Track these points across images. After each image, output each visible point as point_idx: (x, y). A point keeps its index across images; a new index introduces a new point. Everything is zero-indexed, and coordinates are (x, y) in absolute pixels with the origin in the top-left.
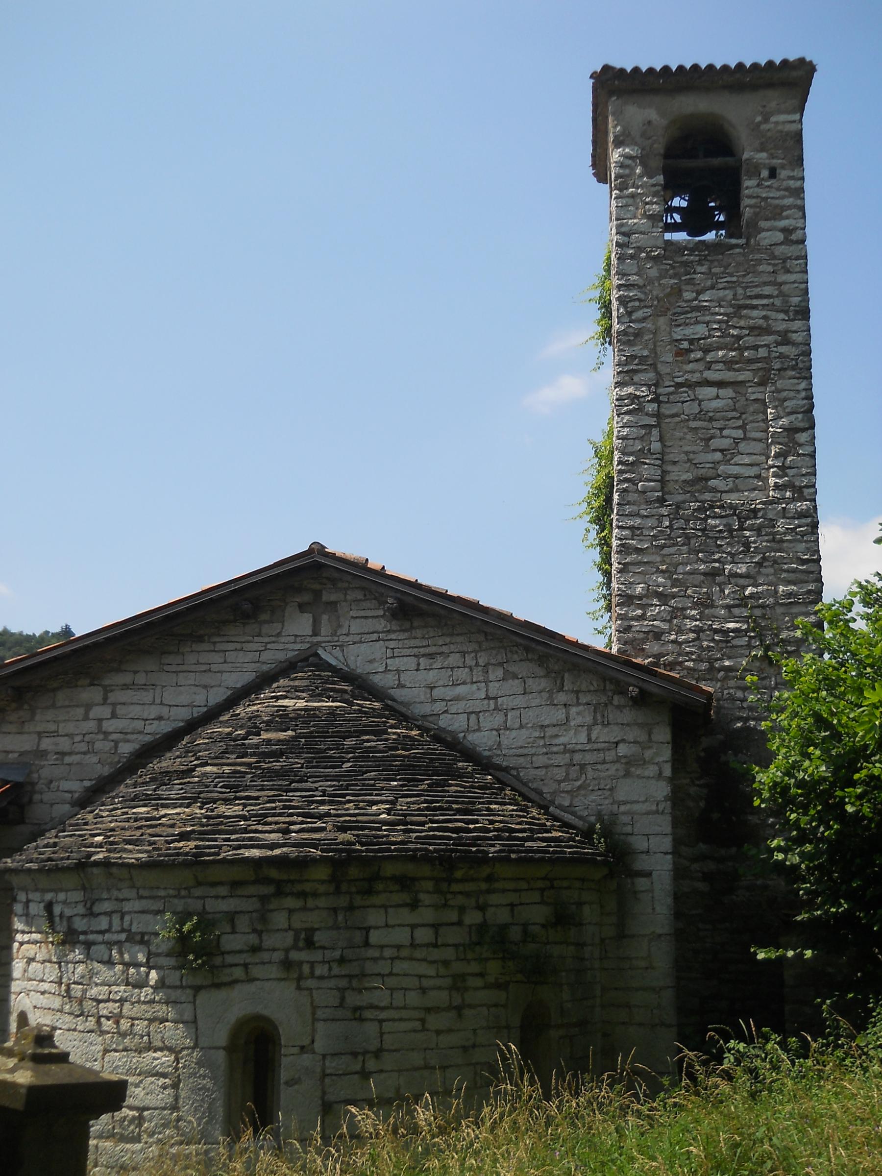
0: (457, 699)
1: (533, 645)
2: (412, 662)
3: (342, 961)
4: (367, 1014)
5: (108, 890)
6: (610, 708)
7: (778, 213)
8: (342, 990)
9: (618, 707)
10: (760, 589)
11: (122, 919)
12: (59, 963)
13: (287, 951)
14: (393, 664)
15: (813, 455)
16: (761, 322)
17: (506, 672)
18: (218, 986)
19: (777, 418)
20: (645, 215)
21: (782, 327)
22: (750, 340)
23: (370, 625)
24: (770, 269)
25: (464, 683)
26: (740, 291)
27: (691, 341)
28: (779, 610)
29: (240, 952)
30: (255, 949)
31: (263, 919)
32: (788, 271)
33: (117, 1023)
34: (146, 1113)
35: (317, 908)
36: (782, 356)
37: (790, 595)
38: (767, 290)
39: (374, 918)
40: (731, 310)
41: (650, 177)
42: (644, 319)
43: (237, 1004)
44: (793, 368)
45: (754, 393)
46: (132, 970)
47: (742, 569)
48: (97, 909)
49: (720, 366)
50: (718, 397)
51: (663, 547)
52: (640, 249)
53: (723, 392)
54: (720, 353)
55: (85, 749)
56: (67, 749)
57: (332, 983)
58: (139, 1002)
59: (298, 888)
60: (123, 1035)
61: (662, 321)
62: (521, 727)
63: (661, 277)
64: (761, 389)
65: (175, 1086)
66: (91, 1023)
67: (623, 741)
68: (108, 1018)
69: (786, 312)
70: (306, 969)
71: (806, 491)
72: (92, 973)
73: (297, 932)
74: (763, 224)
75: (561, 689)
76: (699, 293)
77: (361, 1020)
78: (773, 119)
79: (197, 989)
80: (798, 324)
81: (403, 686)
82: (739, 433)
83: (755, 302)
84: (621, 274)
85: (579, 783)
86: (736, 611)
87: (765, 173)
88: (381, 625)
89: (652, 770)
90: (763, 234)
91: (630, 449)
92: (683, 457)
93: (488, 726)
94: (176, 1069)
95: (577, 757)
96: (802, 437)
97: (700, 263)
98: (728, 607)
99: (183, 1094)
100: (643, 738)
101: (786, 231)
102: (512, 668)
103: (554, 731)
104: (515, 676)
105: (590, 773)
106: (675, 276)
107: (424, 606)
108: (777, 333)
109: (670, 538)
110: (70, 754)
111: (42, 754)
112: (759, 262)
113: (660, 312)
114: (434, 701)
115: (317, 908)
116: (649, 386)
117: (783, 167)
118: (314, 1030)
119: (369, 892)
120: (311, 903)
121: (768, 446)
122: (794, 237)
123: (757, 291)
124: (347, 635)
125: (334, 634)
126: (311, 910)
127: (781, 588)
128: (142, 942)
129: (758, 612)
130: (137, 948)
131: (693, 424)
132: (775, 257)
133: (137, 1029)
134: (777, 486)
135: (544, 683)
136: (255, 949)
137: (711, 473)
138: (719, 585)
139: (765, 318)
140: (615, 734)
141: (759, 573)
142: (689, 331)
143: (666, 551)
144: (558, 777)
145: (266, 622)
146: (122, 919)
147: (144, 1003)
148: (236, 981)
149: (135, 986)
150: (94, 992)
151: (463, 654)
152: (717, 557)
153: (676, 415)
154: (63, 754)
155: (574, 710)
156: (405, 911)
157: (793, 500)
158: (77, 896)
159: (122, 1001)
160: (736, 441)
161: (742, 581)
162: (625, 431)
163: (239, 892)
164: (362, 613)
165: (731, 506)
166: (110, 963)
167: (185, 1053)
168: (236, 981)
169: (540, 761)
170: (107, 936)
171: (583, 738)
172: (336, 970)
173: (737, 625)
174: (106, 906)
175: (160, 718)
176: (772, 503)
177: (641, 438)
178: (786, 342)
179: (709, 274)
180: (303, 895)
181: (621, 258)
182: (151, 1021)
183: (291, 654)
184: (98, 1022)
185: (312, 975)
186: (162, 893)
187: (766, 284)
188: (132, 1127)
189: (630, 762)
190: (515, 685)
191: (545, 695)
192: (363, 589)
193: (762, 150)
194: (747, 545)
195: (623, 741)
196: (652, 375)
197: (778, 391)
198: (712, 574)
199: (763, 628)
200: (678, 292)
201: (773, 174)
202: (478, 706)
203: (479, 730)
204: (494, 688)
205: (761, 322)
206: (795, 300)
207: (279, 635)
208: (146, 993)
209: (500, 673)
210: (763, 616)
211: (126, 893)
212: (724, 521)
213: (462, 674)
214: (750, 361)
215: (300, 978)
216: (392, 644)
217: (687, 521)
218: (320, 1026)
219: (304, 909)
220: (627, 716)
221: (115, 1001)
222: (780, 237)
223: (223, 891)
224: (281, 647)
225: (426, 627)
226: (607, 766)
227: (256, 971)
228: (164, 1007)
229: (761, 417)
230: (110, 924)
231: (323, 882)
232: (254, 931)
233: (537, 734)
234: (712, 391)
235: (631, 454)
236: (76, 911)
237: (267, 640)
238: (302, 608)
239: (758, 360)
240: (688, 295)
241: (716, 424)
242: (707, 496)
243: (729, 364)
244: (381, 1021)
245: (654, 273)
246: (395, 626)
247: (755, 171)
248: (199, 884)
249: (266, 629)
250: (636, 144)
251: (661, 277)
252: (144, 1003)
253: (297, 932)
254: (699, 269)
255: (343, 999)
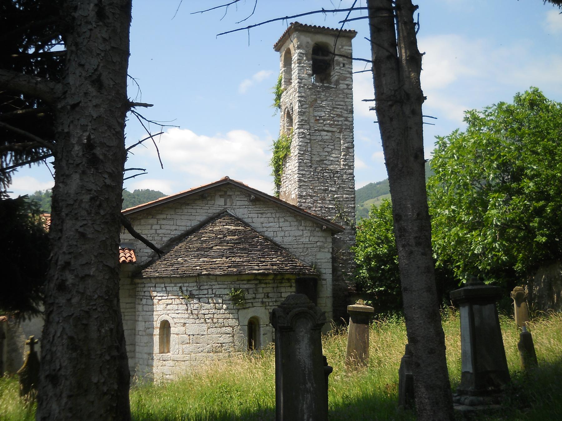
0: (270, 227)
2: (256, 215)
3: (276, 301)
5: (207, 282)
7: (345, 79)
9: (318, 231)
12: (187, 305)
13: (262, 299)
14: (251, 215)
15: (353, 156)
18: (244, 308)
21: (346, 115)
23: (242, 203)
24: (343, 96)
26: (334, 103)
27: (320, 117)
28: (344, 202)
30: (254, 298)
31: (256, 290)
33: (212, 320)
36: (346, 125)
37: (347, 198)
38: (342, 103)
39: (283, 290)
41: (308, 61)
42: (306, 108)
43: (250, 313)
44: (349, 129)
45: (337, 135)
46: (217, 305)
47: (334, 189)
48: (201, 288)
49: (328, 126)
51: (311, 181)
52: (305, 85)
54: (328, 122)
60: (215, 323)
61: (311, 109)
63: (311, 95)
65: (233, 336)
66: (202, 320)
69: (347, 111)
70: (267, 303)
72: (201, 306)
73: (265, 294)
74: (341, 82)
76: (322, 101)
78: (345, 48)
79: (238, 310)
80: (350, 115)
82: (333, 147)
83: (338, 107)
84: (299, 92)
86: (332, 202)
87: (342, 65)
88: (246, 203)
89: (326, 250)
92: (317, 153)
95: (306, 246)
96: (351, 150)
97: (323, 92)
100: (324, 240)
101: (348, 85)
105: (310, 250)
106: (315, 95)
107: (262, 199)
108: (344, 117)
109: (313, 178)
112: (340, 94)
113: (311, 106)
119: (281, 283)
120: (268, 285)
122: (349, 87)
127: (344, 196)
128: (220, 297)
129: (338, 203)
131: (320, 143)
132: (344, 93)
134: (344, 165)
135: (296, 223)
136: (254, 298)
137: (325, 159)
140: (316, 239)
142: (319, 114)
148: (249, 307)
150: (203, 312)
155: (305, 232)
157: (348, 169)
159: (214, 314)
161: (334, 193)
165: (331, 170)
166: (209, 303)
168: (249, 307)
169: (295, 246)
174: (206, 287)
175: (176, 230)
176: (342, 169)
178: (346, 120)
179: (325, 95)
180: (266, 283)
181: (299, 87)
183: (218, 211)
184: (205, 320)
185: (269, 305)
189: (321, 247)
190: (287, 224)
191: (296, 227)
192: (241, 191)
194: (335, 182)
196: (308, 127)
197: (345, 135)
199: (340, 208)
200: (316, 100)
201: (344, 66)
202: (276, 229)
204: (281, 224)
206: (350, 107)
207: (213, 204)
208: (222, 311)
209: (283, 220)
213: (272, 220)
214: (337, 125)
215: (266, 306)
216: (250, 209)
217: (318, 173)
219: (266, 287)
220: (320, 234)
222: (346, 87)
223: (245, 282)
229: (339, 143)
230: (208, 292)
234: (325, 133)
238: (221, 196)
239: (339, 125)
240: (319, 102)
241: (327, 144)
242: (324, 166)
243: (330, 125)
245: (309, 93)
247: (338, 64)
248: (238, 280)
249: (209, 202)
251: (311, 95)
253: (265, 294)
254: (323, 94)
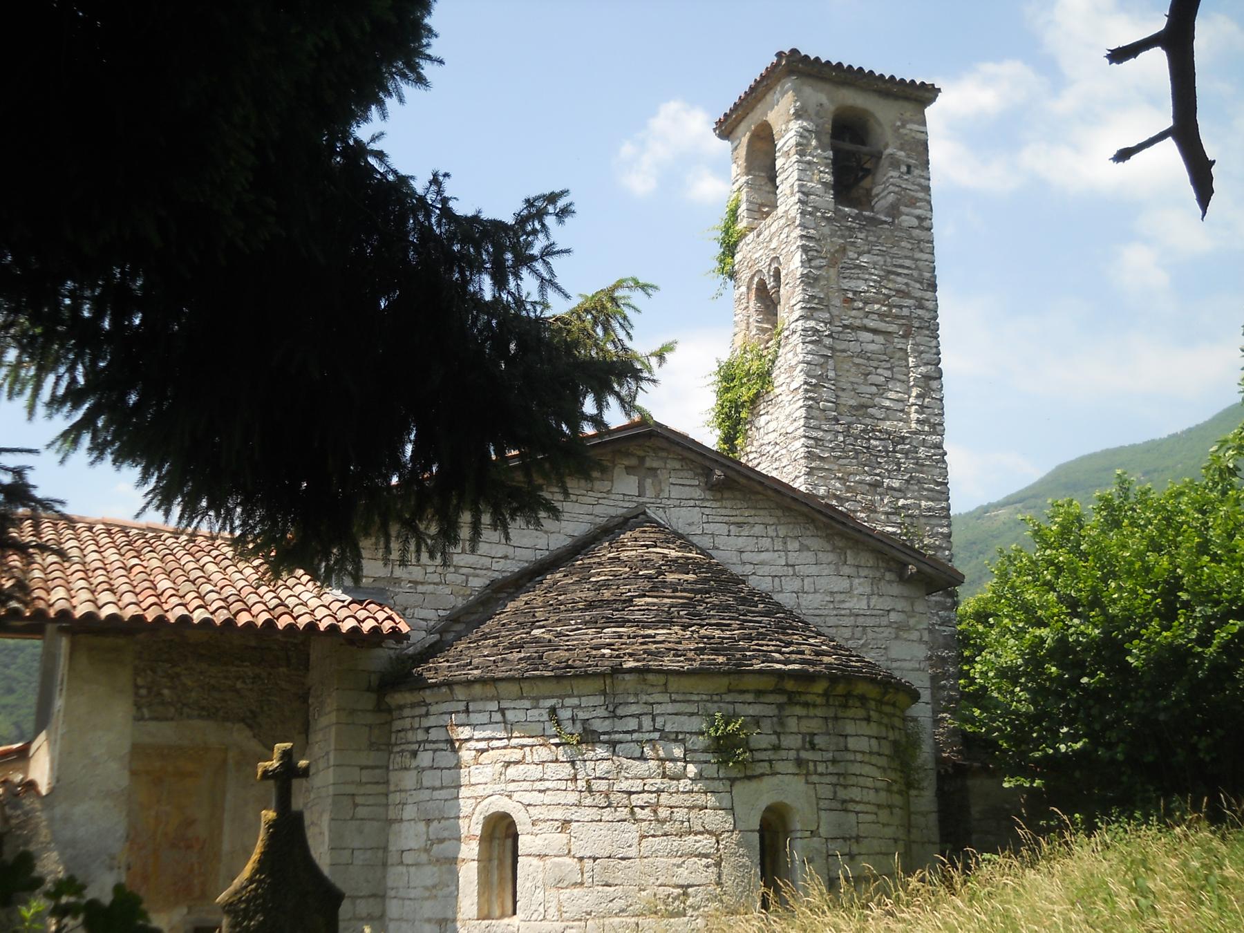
0: (762, 563)
1: (834, 524)
2: (723, 529)
3: (834, 761)
4: (851, 806)
5: (636, 695)
6: (882, 583)
7: (913, 203)
8: (835, 785)
9: (889, 582)
10: (909, 502)
11: (654, 720)
12: (573, 763)
13: (798, 750)
14: (710, 528)
15: (941, 400)
16: (904, 287)
17: (801, 544)
18: (750, 778)
19: (917, 366)
20: (820, 181)
21: (919, 294)
22: (895, 300)
23: (687, 492)
24: (910, 246)
25: (767, 550)
26: (889, 260)
27: (855, 293)
28: (923, 520)
29: (765, 750)
30: (776, 748)
31: (782, 724)
32: (922, 251)
33: (655, 812)
34: (690, 890)
35: (816, 716)
36: (919, 317)
37: (930, 509)
38: (908, 263)
39: (850, 728)
40: (882, 273)
41: (824, 151)
42: (820, 268)
43: (765, 793)
44: (928, 328)
45: (898, 343)
46: (669, 764)
47: (896, 484)
48: (620, 712)
49: (875, 317)
50: (873, 342)
51: (839, 458)
52: (816, 209)
53: (876, 338)
54: (876, 307)
55: (438, 580)
56: (420, 579)
57: (828, 779)
58: (676, 793)
59: (803, 699)
60: (664, 822)
61: (833, 272)
62: (815, 592)
63: (832, 236)
64: (904, 341)
65: (718, 865)
66: (623, 813)
67: (893, 609)
68: (642, 808)
69: (921, 283)
70: (811, 764)
71: (939, 428)
72: (620, 768)
73: (804, 735)
74: (903, 209)
75: (845, 563)
76: (860, 254)
77: (846, 810)
78: (909, 126)
79: (733, 781)
80: (929, 295)
81: (718, 549)
82: (888, 374)
83: (900, 270)
84: (803, 226)
85: (861, 642)
86: (893, 518)
87: (904, 169)
88: (697, 493)
89: (915, 635)
90: (904, 217)
91: (812, 373)
92: (849, 386)
93: (789, 588)
94: (718, 850)
95: (861, 620)
96: (934, 384)
97: (860, 230)
98: (887, 514)
99: (725, 871)
100: (908, 608)
101: (920, 219)
102: (808, 542)
103: (842, 597)
104: (808, 549)
105: (870, 634)
106: (842, 237)
107: (743, 481)
108: (915, 298)
109: (843, 451)
110: (422, 583)
111: (397, 581)
112: (901, 239)
113: (832, 263)
114: (744, 563)
115: (816, 716)
116: (826, 324)
117: (916, 167)
118: (819, 817)
119: (845, 706)
120: (812, 712)
121: (910, 388)
122: (925, 224)
123: (900, 262)
124: (668, 499)
125: (657, 497)
126: (812, 718)
127: (923, 503)
128: (676, 740)
129: (908, 520)
130: (672, 745)
131: (857, 361)
132: (912, 238)
133: (676, 816)
134: (918, 421)
135: (831, 557)
136: (776, 748)
137: (869, 403)
138: (880, 494)
139: (906, 284)
140: (886, 603)
141: (907, 488)
142: (853, 284)
143: (841, 461)
144: (846, 636)
145: (597, 479)
146: (654, 720)
147: (683, 792)
148: (763, 775)
149: (672, 779)
150: (625, 785)
151: (766, 525)
152: (878, 471)
153: (844, 351)
154: (416, 583)
155: (857, 581)
156: (864, 723)
157: (929, 433)
158: (600, 700)
159: (659, 792)
160: (888, 379)
161: (896, 494)
162: (809, 357)
163: (762, 700)
164: (680, 481)
165: (887, 432)
166: (642, 758)
167: (726, 835)
168: (763, 775)
169: (832, 621)
170: (635, 736)
171: (863, 605)
172: (831, 769)
173: (894, 529)
174: (634, 709)
175: (506, 557)
176: (915, 433)
177: (821, 365)
178: (921, 307)
179: (866, 239)
180: (806, 705)
181: (803, 213)
182: (691, 808)
183: (620, 511)
184: (632, 812)
185: (815, 773)
186: (695, 698)
187: (906, 257)
188: (677, 903)
189: (900, 628)
190: (808, 557)
191: (833, 567)
192: (683, 459)
193: (901, 149)
194: (898, 464)
195: (893, 609)
196: (827, 315)
197: (917, 344)
198: (875, 485)
199: (914, 534)
200: (843, 250)
201: (909, 172)
202: (780, 571)
203: (781, 592)
204: (793, 558)
205: (904, 287)
206: (927, 275)
207: (609, 492)
208: (684, 784)
209: (796, 545)
210: (912, 524)
211: (657, 697)
212: (883, 443)
213: (766, 543)
214: (897, 317)
215: (808, 774)
216: (707, 511)
217: (856, 439)
218: (822, 813)
219: (807, 717)
220: (895, 589)
221: (652, 792)
222: (915, 222)
223: (749, 697)
224: (612, 503)
225: (734, 499)
226: (881, 629)
227: (779, 767)
228: (703, 796)
229: (904, 363)
230: (640, 726)
231: (819, 695)
232: (775, 733)
233: (828, 599)
234: (869, 336)
235: (813, 377)
236: (595, 714)
237: (600, 495)
238: (629, 470)
239: (903, 317)
240: (852, 255)
241: (875, 364)
242: (868, 421)
243: (882, 316)
244: (857, 813)
245: (827, 230)
246: (709, 495)
247: (895, 164)
248: (729, 691)
249: (597, 484)
250: (811, 120)
251: (832, 236)
252: (683, 792)
253: (804, 735)
254: (860, 235)
255: (835, 793)
